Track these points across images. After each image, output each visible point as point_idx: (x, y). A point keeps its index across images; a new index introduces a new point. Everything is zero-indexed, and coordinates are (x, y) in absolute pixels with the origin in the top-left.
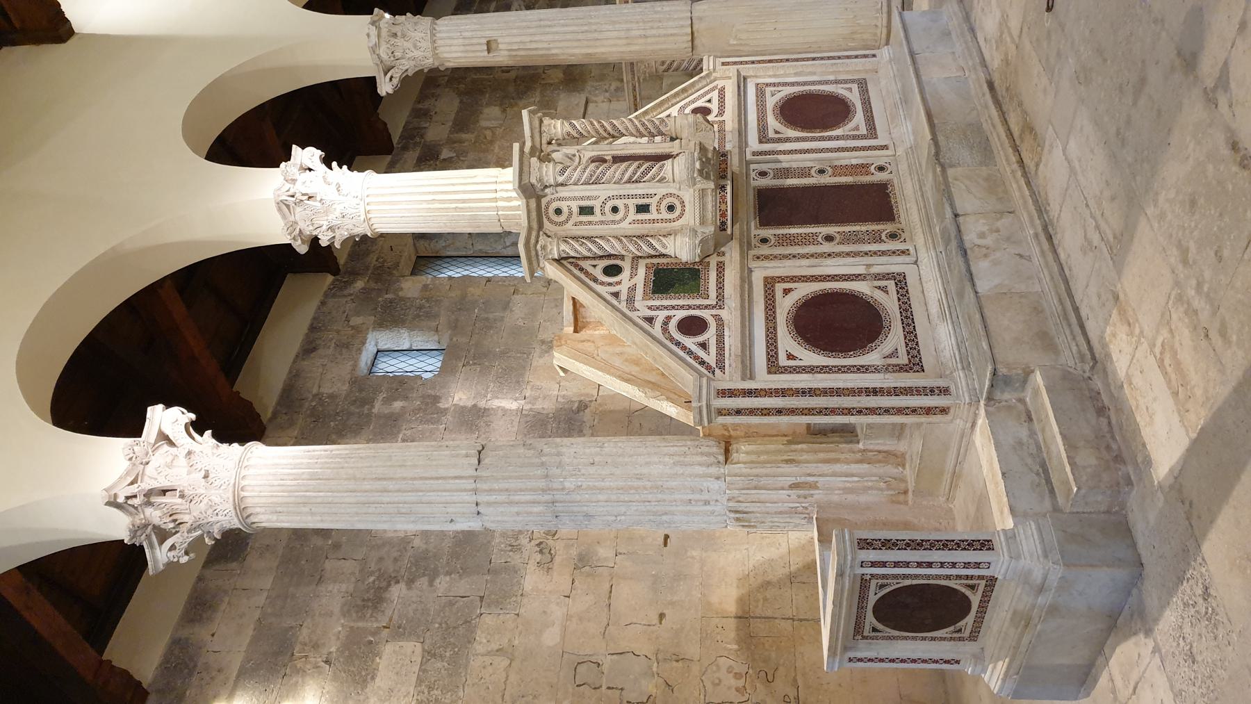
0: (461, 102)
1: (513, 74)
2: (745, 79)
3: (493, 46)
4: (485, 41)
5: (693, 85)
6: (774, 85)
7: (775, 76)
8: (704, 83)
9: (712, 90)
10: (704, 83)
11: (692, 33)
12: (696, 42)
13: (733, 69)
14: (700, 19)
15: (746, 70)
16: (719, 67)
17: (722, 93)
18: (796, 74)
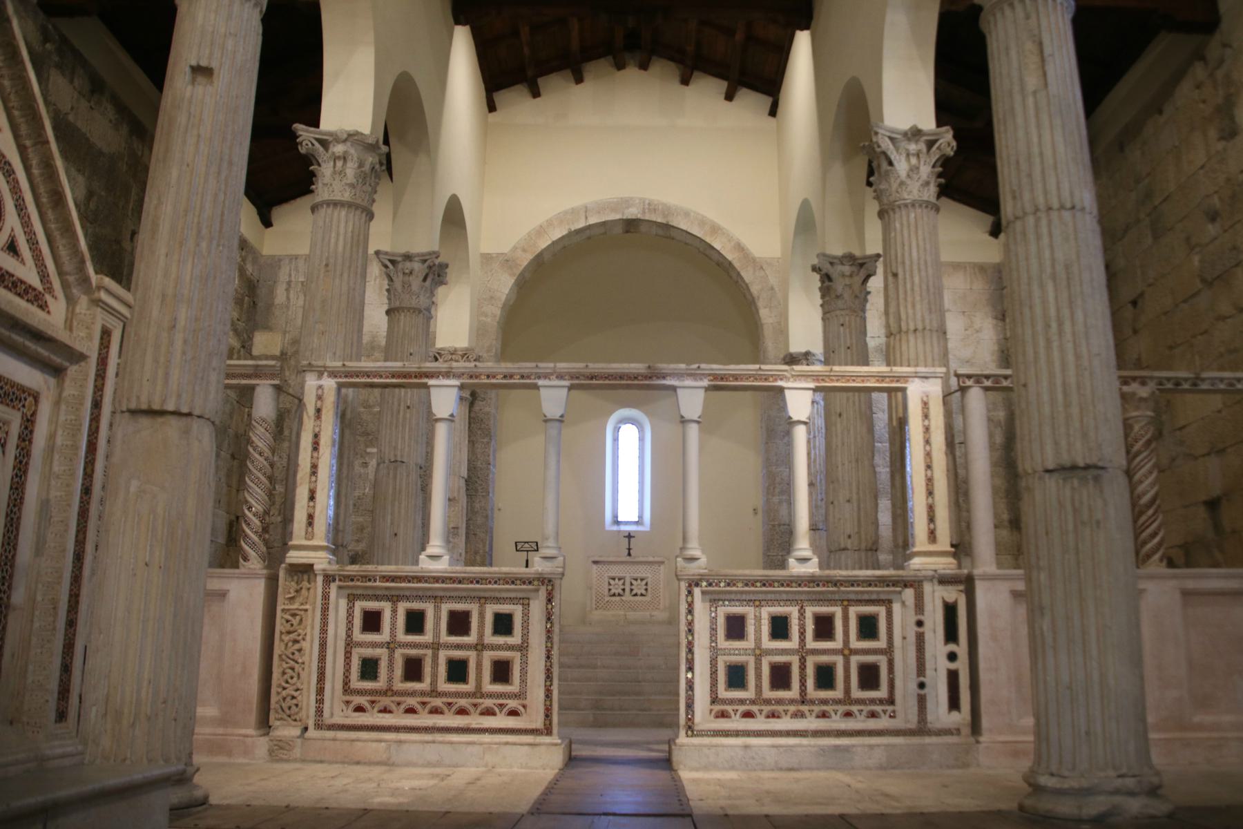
0: (101, 153)
1: (126, 245)
2: (58, 372)
3: (200, 79)
4: (214, 64)
5: (68, 229)
6: (26, 436)
7: (50, 449)
8: (68, 267)
9: (44, 276)
10: (68, 267)
11: (162, 413)
12: (145, 421)
13: (91, 349)
14: (186, 432)
15: (80, 378)
16: (100, 319)
17: (37, 299)
18: (45, 505)
